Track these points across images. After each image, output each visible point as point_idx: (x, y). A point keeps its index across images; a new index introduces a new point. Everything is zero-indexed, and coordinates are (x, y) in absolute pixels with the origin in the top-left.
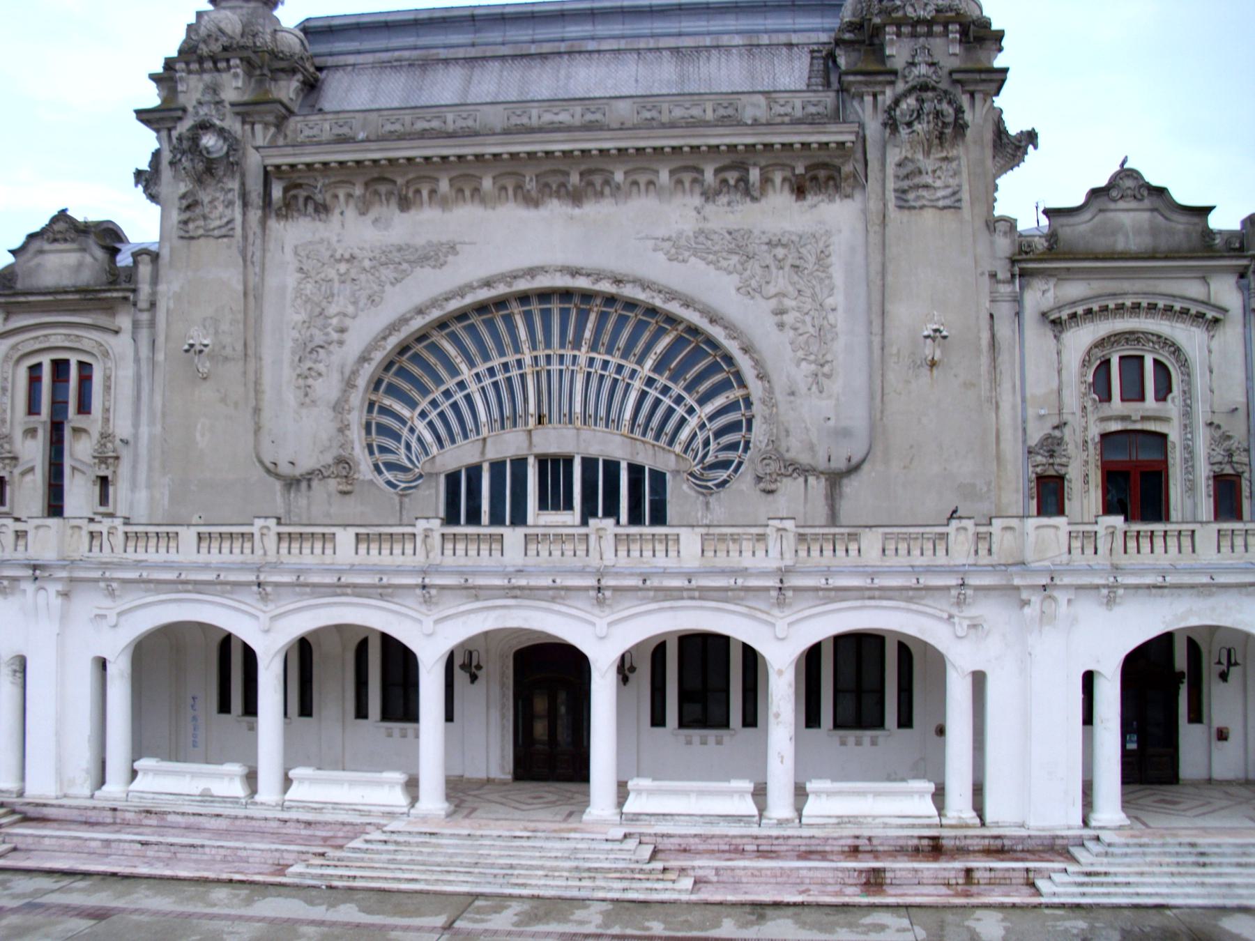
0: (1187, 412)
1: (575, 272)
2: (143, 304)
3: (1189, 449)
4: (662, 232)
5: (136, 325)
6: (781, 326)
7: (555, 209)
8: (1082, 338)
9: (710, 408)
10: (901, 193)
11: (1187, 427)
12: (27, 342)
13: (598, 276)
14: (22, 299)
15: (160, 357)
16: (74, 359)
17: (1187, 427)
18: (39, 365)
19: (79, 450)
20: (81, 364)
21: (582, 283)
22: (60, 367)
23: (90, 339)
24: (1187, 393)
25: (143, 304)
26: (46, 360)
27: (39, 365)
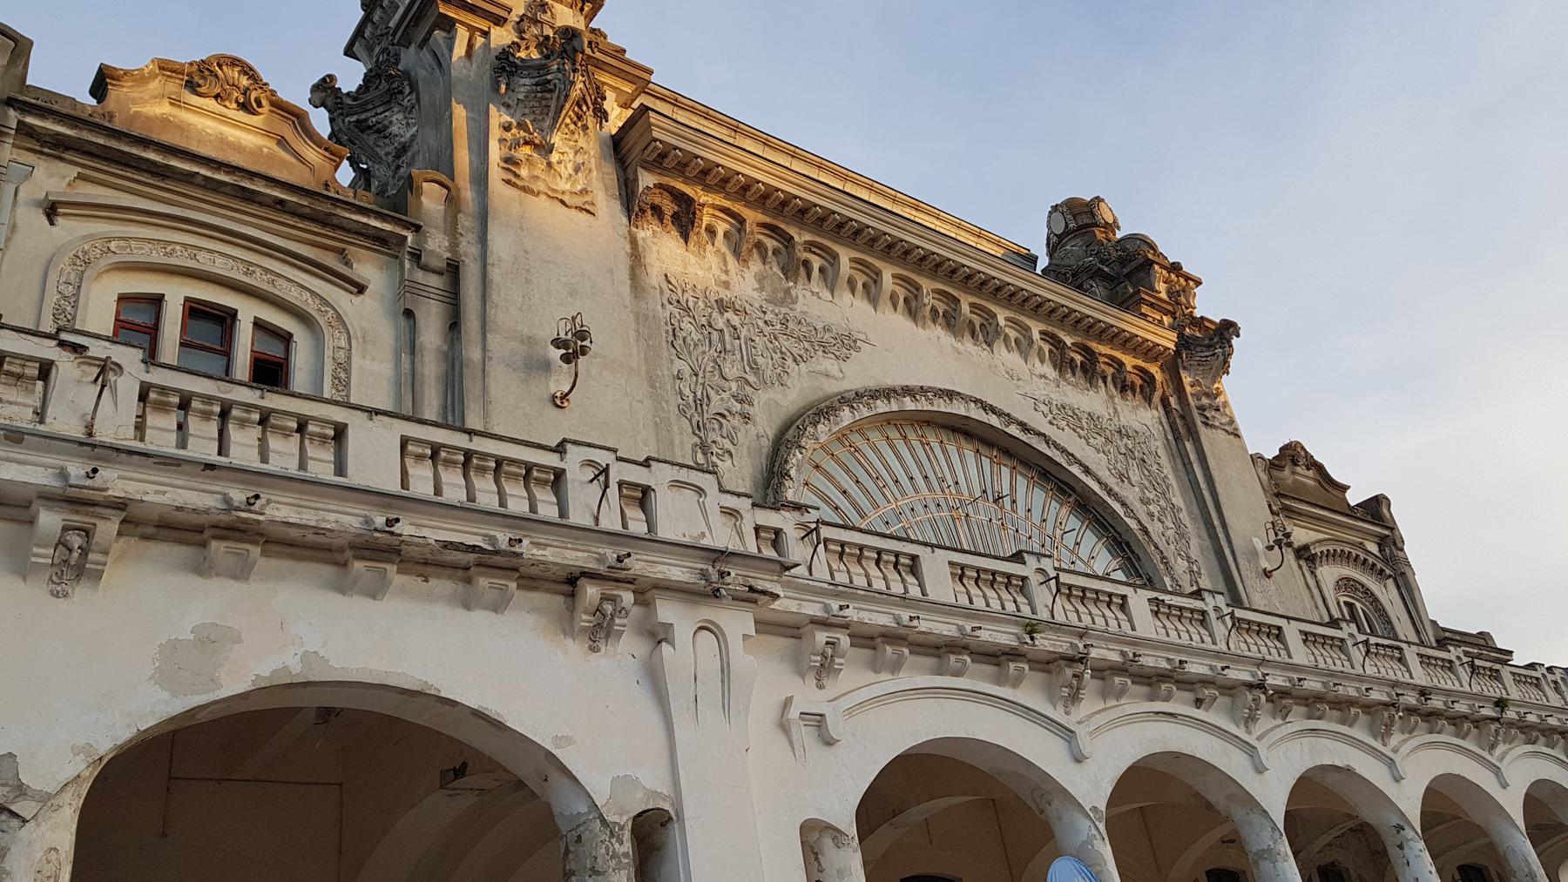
6: (1151, 515)
7: (938, 332)
8: (1329, 574)
12: (145, 241)
13: (1009, 418)
14: (152, 156)
18: (157, 301)
20: (259, 325)
23: (297, 285)
26: (176, 294)
27: (157, 301)
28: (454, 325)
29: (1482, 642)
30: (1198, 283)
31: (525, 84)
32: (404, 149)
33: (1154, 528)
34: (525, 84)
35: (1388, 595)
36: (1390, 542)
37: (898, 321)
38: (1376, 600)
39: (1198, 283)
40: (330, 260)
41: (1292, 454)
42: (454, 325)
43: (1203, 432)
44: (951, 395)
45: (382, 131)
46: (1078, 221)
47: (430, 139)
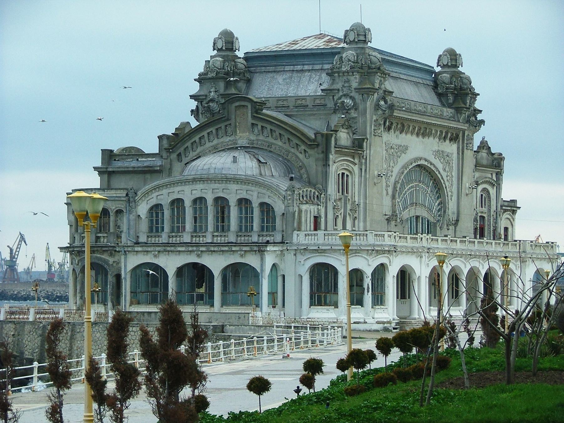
0: (489, 210)
1: (426, 160)
2: (365, 157)
3: (489, 220)
4: (434, 150)
5: (361, 164)
8: (480, 188)
9: (437, 204)
10: (467, 144)
11: (489, 216)
15: (368, 176)
16: (346, 173)
17: (489, 216)
19: (349, 207)
21: (426, 163)
22: (343, 174)
24: (490, 206)
25: (365, 157)
26: (341, 172)
28: (366, 170)
29: (513, 204)
30: (479, 94)
31: (380, 112)
32: (354, 118)
33: (447, 184)
34: (380, 112)
35: (492, 191)
36: (499, 175)
37: (414, 137)
38: (489, 194)
39: (479, 94)
40: (353, 160)
41: (484, 145)
42: (366, 170)
43: (465, 151)
44: (421, 159)
45: (349, 114)
46: (452, 59)
47: (361, 120)
